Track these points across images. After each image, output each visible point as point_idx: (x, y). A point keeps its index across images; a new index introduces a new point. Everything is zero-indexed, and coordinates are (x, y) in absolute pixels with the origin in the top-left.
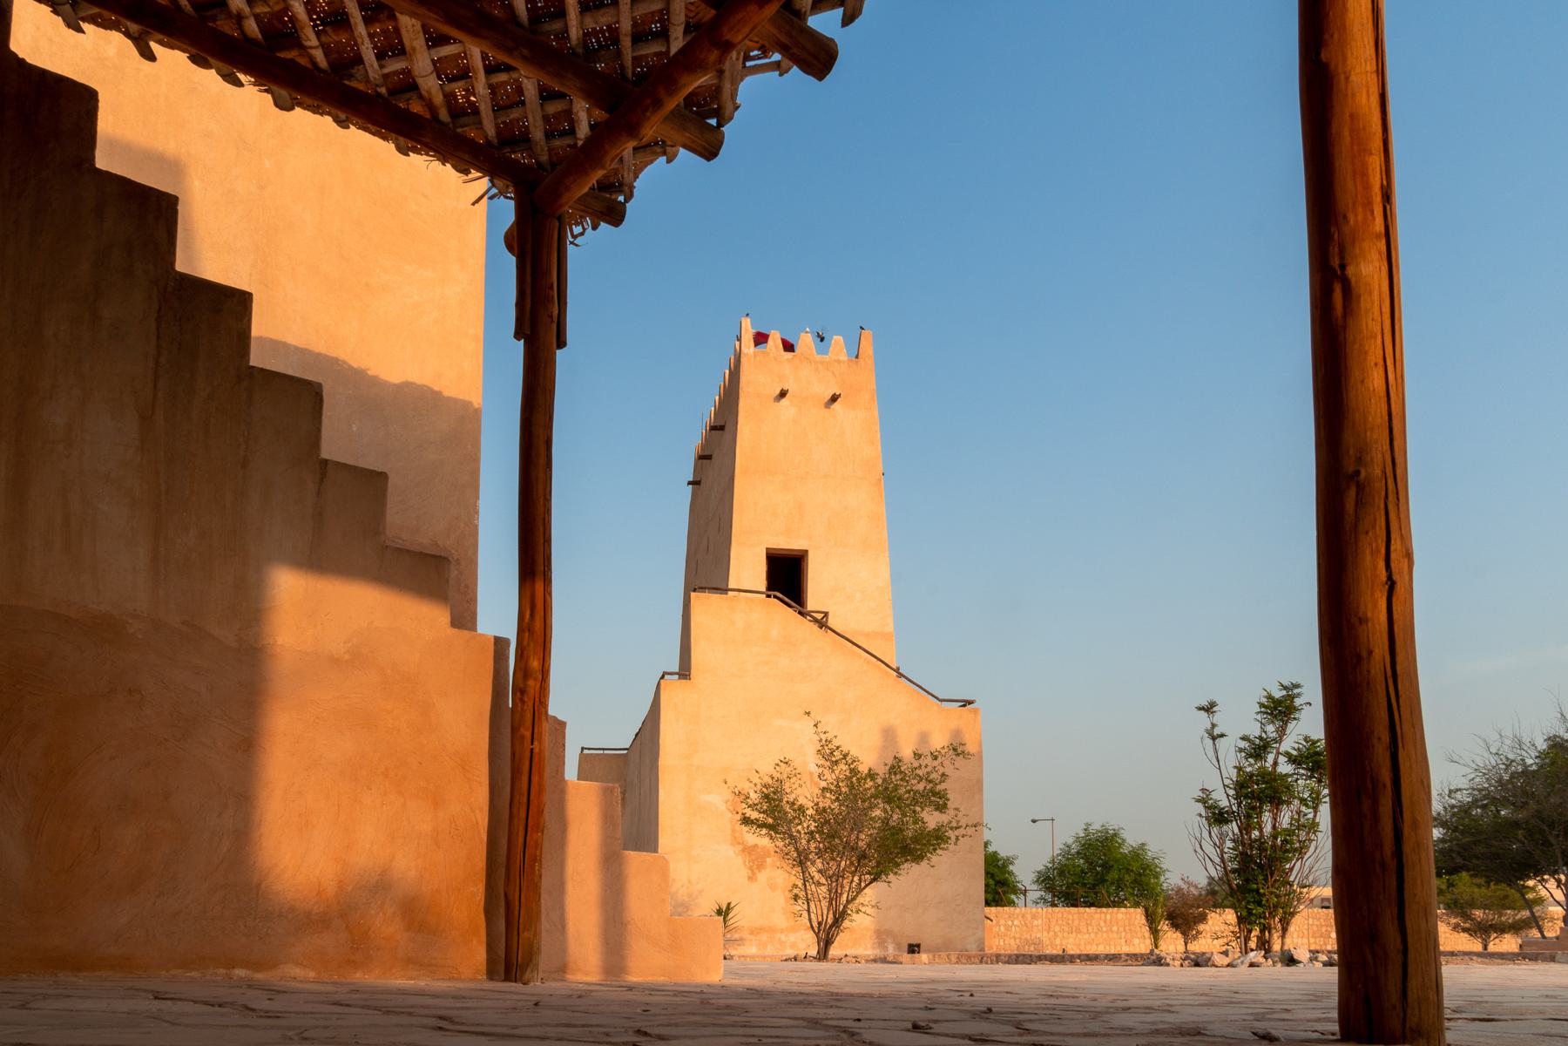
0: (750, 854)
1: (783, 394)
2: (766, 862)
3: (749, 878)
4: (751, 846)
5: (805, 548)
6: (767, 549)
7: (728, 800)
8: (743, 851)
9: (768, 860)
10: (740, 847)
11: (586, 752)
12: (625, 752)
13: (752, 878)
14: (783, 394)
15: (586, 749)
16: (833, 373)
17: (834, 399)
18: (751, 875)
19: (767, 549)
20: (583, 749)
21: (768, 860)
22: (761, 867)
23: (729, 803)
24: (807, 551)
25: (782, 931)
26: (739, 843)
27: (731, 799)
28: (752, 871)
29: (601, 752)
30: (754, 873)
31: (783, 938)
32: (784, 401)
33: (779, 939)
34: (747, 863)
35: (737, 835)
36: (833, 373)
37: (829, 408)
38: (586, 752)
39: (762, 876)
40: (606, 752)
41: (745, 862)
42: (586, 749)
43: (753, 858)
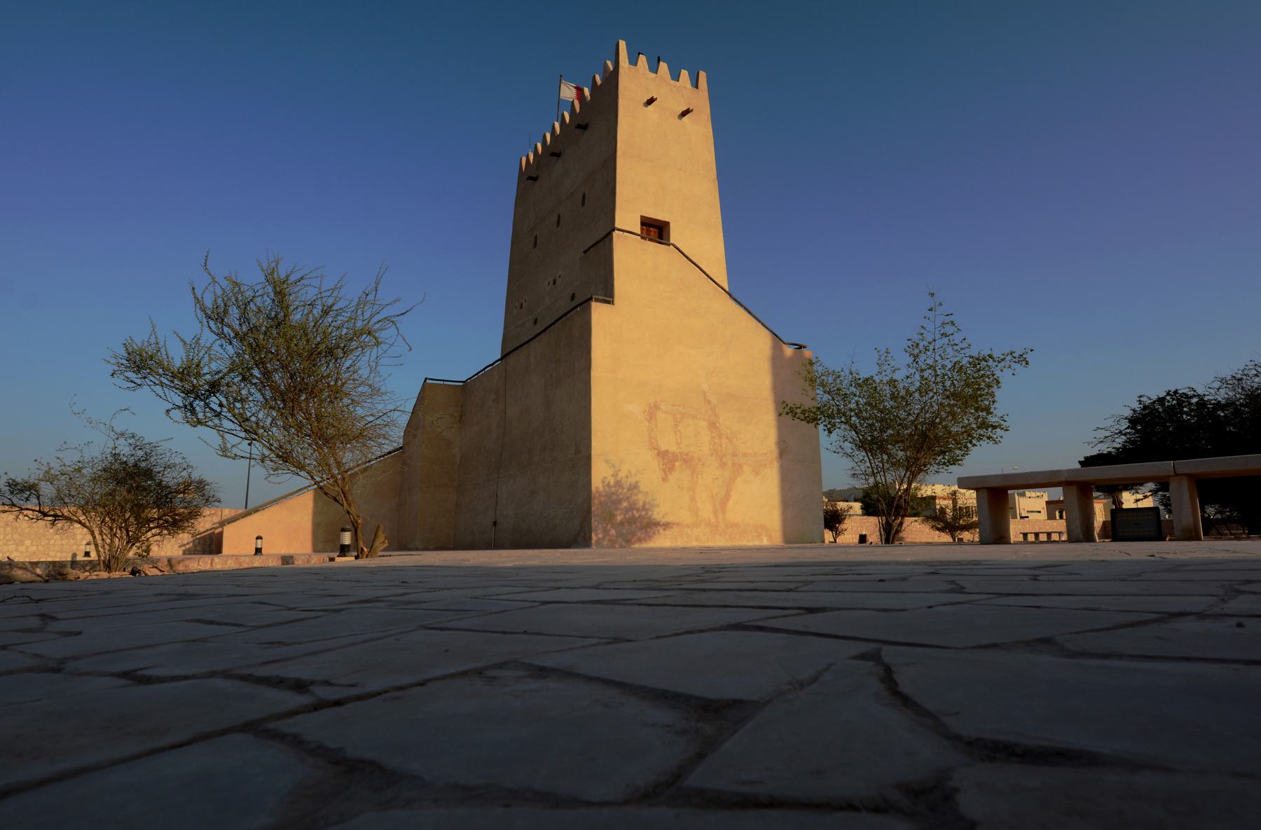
0: (663, 458)
1: (650, 101)
2: (674, 465)
6: (641, 216)
9: (677, 464)
10: (656, 451)
12: (462, 384)
13: (665, 479)
14: (650, 101)
15: (429, 379)
17: (684, 114)
19: (641, 216)
20: (426, 379)
22: (672, 469)
24: (667, 224)
25: (688, 526)
26: (654, 448)
28: (665, 472)
29: (442, 382)
30: (666, 475)
31: (690, 532)
35: (653, 440)
37: (681, 119)
38: (428, 381)
39: (672, 477)
40: (445, 383)
41: (659, 466)
42: (429, 379)
43: (666, 461)
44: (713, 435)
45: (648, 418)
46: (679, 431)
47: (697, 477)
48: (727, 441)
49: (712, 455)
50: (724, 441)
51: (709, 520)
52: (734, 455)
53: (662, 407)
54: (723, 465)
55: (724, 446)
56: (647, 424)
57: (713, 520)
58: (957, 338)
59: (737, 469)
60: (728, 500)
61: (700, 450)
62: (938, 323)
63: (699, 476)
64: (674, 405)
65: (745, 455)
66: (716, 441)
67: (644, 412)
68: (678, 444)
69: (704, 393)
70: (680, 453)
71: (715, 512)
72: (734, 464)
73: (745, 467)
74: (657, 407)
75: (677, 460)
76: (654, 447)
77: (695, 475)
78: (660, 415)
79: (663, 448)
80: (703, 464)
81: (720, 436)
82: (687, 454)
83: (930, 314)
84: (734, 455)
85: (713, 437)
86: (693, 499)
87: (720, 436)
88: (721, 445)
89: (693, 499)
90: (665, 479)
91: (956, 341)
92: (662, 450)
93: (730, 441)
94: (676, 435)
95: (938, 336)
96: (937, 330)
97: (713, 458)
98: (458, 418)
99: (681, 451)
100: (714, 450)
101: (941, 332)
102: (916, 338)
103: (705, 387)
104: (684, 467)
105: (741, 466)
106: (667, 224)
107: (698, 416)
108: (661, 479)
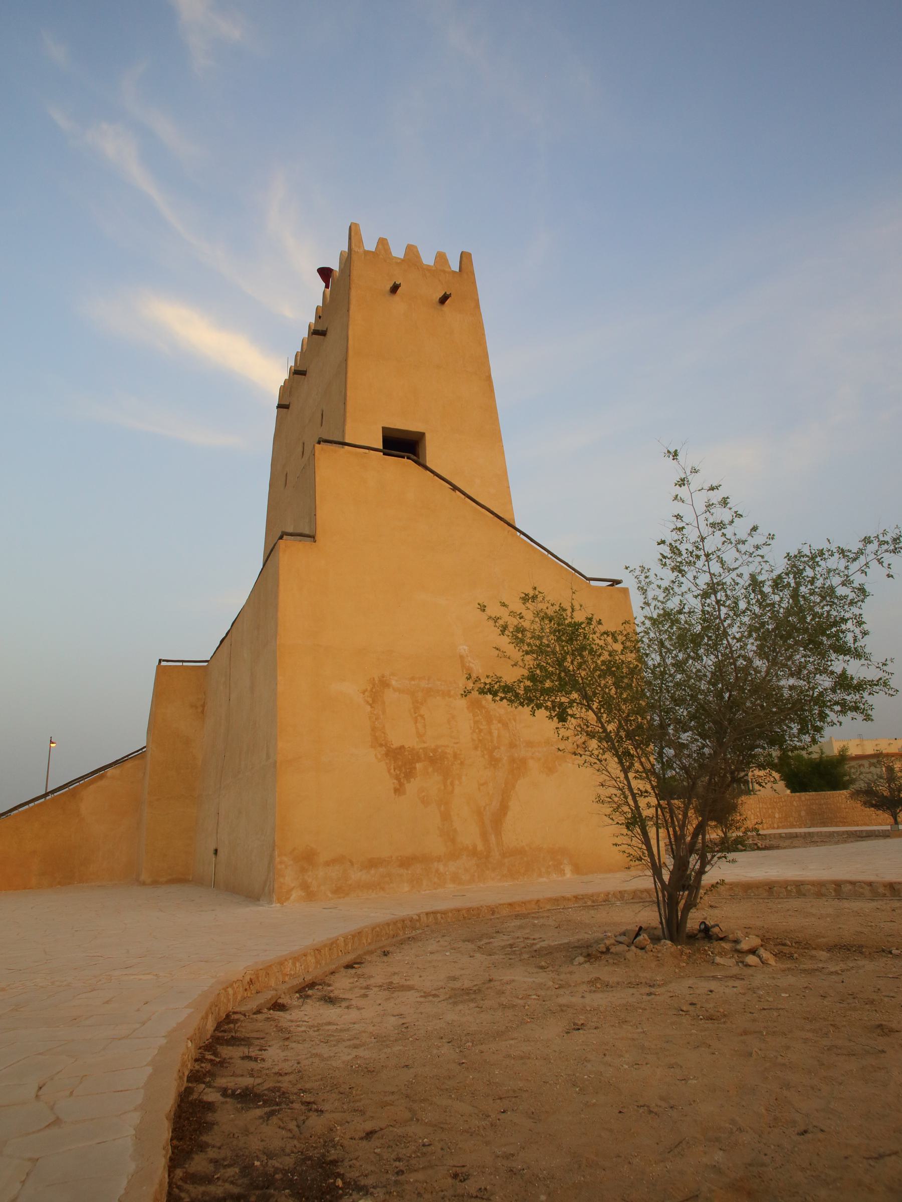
1: (395, 289)
2: (415, 768)
3: (396, 791)
4: (396, 749)
5: (422, 431)
6: (383, 428)
7: (366, 690)
8: (387, 755)
9: (418, 766)
10: (383, 750)
11: (163, 663)
12: (205, 664)
13: (399, 791)
15: (164, 661)
16: (440, 280)
17: (444, 300)
18: (398, 787)
19: (383, 428)
20: (160, 661)
21: (418, 766)
22: (410, 774)
23: (367, 694)
24: (422, 435)
25: (439, 859)
26: (381, 745)
27: (369, 689)
28: (397, 778)
29: (180, 664)
30: (401, 784)
31: (442, 868)
32: (397, 297)
33: (437, 870)
34: (392, 771)
36: (440, 280)
38: (163, 663)
39: (412, 787)
40: (185, 664)
41: (389, 771)
42: (164, 661)
43: (400, 763)
44: (477, 718)
45: (370, 700)
46: (422, 716)
47: (452, 784)
48: (500, 725)
49: (476, 748)
50: (496, 727)
51: (475, 847)
52: (512, 745)
53: (394, 683)
54: (494, 762)
55: (495, 733)
56: (368, 708)
57: (480, 847)
58: (741, 529)
59: (518, 767)
60: (505, 814)
61: (457, 743)
62: (701, 507)
63: (457, 782)
64: (413, 679)
65: (530, 744)
66: (482, 727)
67: (364, 693)
68: (420, 736)
69: (462, 657)
70: (424, 749)
71: (484, 836)
72: (512, 760)
73: (531, 763)
74: (384, 683)
75: (419, 760)
76: (378, 740)
77: (449, 781)
78: (390, 696)
79: (396, 744)
80: (462, 763)
81: (489, 720)
82: (435, 751)
83: (683, 492)
84: (512, 745)
85: (476, 722)
86: (446, 817)
87: (489, 720)
88: (490, 733)
89: (446, 817)
90: (399, 791)
91: (743, 534)
92: (394, 746)
93: (505, 725)
94: (416, 722)
95: (706, 530)
96: (701, 519)
97: (479, 753)
98: (200, 710)
99: (425, 745)
100: (480, 740)
101: (711, 520)
102: (670, 537)
103: (463, 649)
104: (430, 769)
105: (524, 761)
106: (422, 435)
107: (452, 693)
108: (392, 791)
